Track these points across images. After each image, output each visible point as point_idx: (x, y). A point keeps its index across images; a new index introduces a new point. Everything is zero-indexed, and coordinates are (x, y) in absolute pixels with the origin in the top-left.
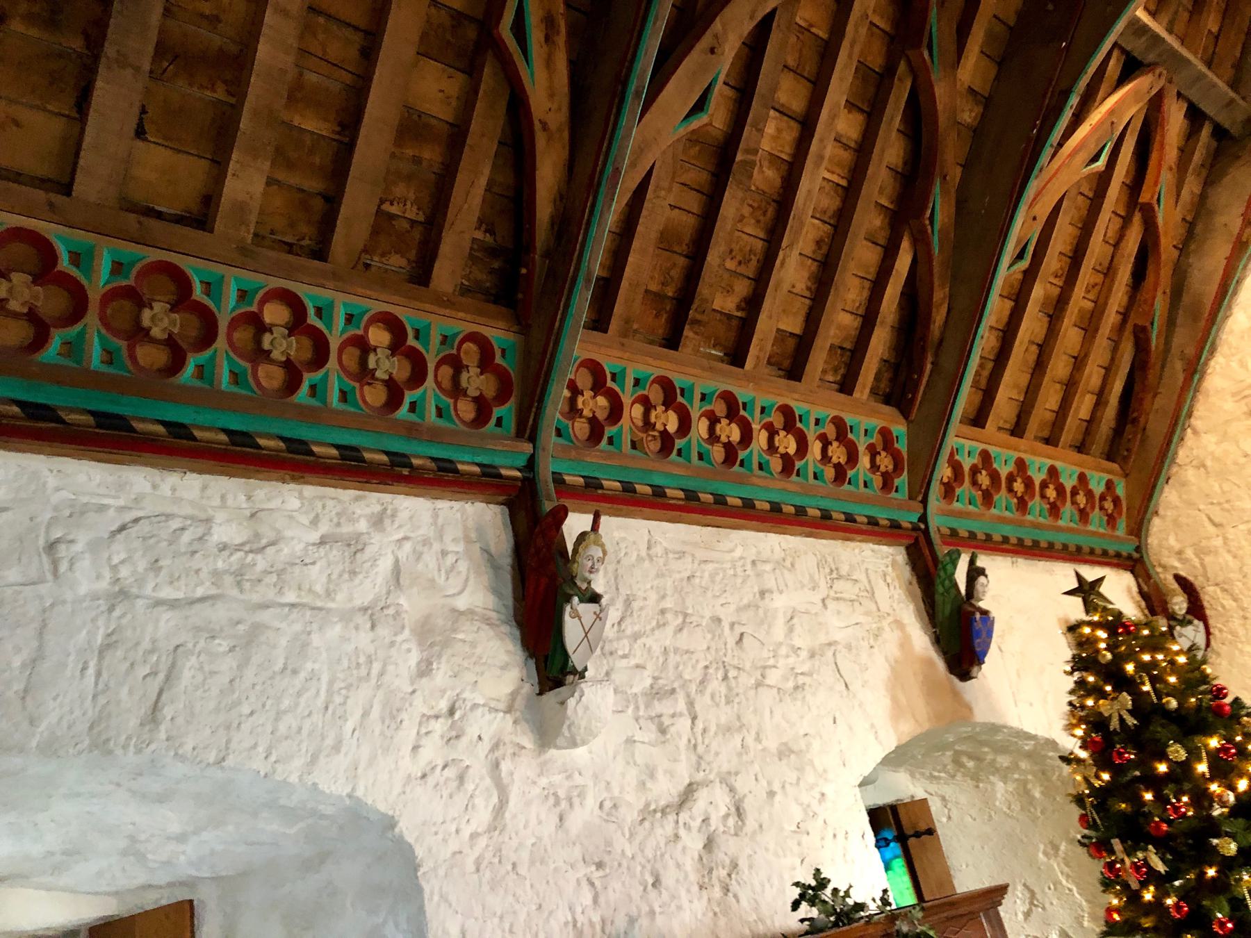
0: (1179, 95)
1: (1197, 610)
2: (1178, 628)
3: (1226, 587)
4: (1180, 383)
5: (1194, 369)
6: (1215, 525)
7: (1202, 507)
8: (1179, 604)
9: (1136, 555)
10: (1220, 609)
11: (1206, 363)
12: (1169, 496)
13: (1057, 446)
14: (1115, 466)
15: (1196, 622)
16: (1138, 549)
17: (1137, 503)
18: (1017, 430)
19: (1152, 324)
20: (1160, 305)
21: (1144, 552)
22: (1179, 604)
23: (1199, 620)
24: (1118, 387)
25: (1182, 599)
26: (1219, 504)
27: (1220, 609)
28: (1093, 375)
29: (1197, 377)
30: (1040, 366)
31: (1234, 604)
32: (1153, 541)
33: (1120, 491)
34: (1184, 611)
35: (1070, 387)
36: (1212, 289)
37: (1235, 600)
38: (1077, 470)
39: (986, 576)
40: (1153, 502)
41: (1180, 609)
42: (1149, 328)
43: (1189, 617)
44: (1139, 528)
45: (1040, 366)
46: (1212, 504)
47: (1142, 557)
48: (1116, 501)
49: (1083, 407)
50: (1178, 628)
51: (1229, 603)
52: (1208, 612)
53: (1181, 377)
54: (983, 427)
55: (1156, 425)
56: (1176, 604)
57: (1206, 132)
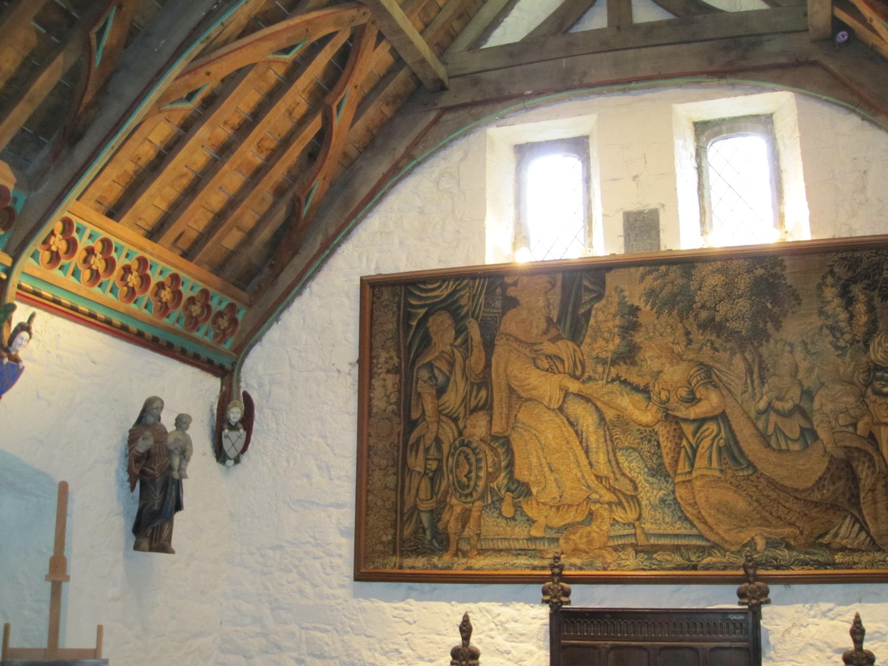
0: (381, 37)
1: (247, 421)
2: (226, 431)
3: (276, 413)
4: (315, 251)
5: (329, 247)
6: (291, 366)
7: (289, 349)
8: (235, 414)
9: (228, 366)
10: (266, 427)
11: (339, 245)
12: (274, 334)
13: (191, 260)
14: (245, 295)
15: (242, 431)
16: (233, 364)
17: (248, 329)
18: (154, 234)
19: (307, 199)
20: (318, 186)
21: (237, 367)
22: (235, 414)
23: (245, 429)
24: (265, 234)
25: (239, 411)
26: (300, 351)
27: (266, 427)
28: (248, 216)
29: (327, 252)
30: (192, 190)
31: (274, 426)
32: (248, 362)
33: (240, 316)
34: (237, 420)
35: (220, 218)
36: (364, 191)
37: (278, 424)
38: (201, 286)
39: (30, 334)
40: (259, 333)
41: (234, 418)
42: (303, 199)
43: (240, 425)
44: (243, 349)
45: (192, 190)
46: (296, 349)
47: (233, 370)
48: (234, 322)
49: (231, 239)
50: (226, 431)
51: (273, 425)
52: (255, 426)
53: (318, 246)
54: (118, 221)
55: (287, 277)
56: (233, 413)
57: (402, 75)
